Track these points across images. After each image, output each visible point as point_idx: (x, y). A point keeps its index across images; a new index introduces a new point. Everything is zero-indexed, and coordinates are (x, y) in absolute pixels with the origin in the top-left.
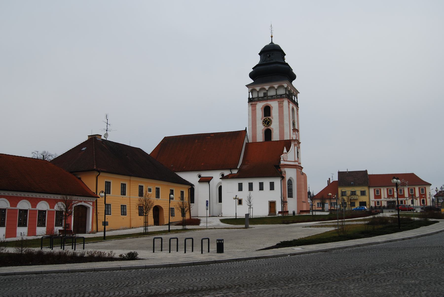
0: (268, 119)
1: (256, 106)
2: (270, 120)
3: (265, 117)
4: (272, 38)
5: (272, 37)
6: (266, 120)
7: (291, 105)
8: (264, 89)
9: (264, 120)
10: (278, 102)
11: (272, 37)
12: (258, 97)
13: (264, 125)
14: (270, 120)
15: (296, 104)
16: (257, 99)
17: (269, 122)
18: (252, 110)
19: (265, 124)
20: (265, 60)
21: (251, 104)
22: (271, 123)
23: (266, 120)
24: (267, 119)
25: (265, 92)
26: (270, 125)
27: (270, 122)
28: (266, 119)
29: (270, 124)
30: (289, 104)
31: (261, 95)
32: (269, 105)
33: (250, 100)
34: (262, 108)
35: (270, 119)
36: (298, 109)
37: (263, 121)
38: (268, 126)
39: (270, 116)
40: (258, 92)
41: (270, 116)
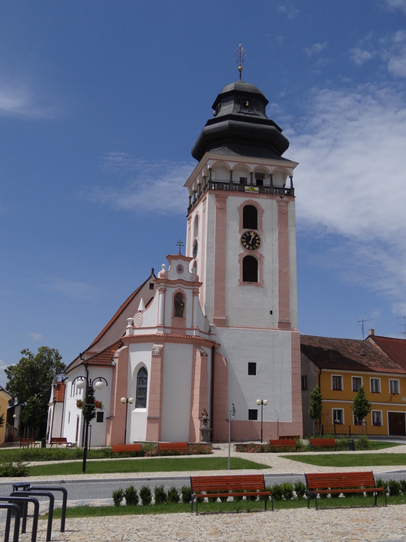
1: (226, 202)
6: (248, 235)
9: (245, 234)
10: (277, 201)
13: (245, 246)
18: (217, 208)
22: (259, 243)
23: (248, 235)
27: (257, 241)
28: (249, 233)
29: (257, 245)
34: (239, 209)
37: (243, 238)
38: (253, 249)
39: (256, 228)
40: (231, 171)
41: (256, 228)
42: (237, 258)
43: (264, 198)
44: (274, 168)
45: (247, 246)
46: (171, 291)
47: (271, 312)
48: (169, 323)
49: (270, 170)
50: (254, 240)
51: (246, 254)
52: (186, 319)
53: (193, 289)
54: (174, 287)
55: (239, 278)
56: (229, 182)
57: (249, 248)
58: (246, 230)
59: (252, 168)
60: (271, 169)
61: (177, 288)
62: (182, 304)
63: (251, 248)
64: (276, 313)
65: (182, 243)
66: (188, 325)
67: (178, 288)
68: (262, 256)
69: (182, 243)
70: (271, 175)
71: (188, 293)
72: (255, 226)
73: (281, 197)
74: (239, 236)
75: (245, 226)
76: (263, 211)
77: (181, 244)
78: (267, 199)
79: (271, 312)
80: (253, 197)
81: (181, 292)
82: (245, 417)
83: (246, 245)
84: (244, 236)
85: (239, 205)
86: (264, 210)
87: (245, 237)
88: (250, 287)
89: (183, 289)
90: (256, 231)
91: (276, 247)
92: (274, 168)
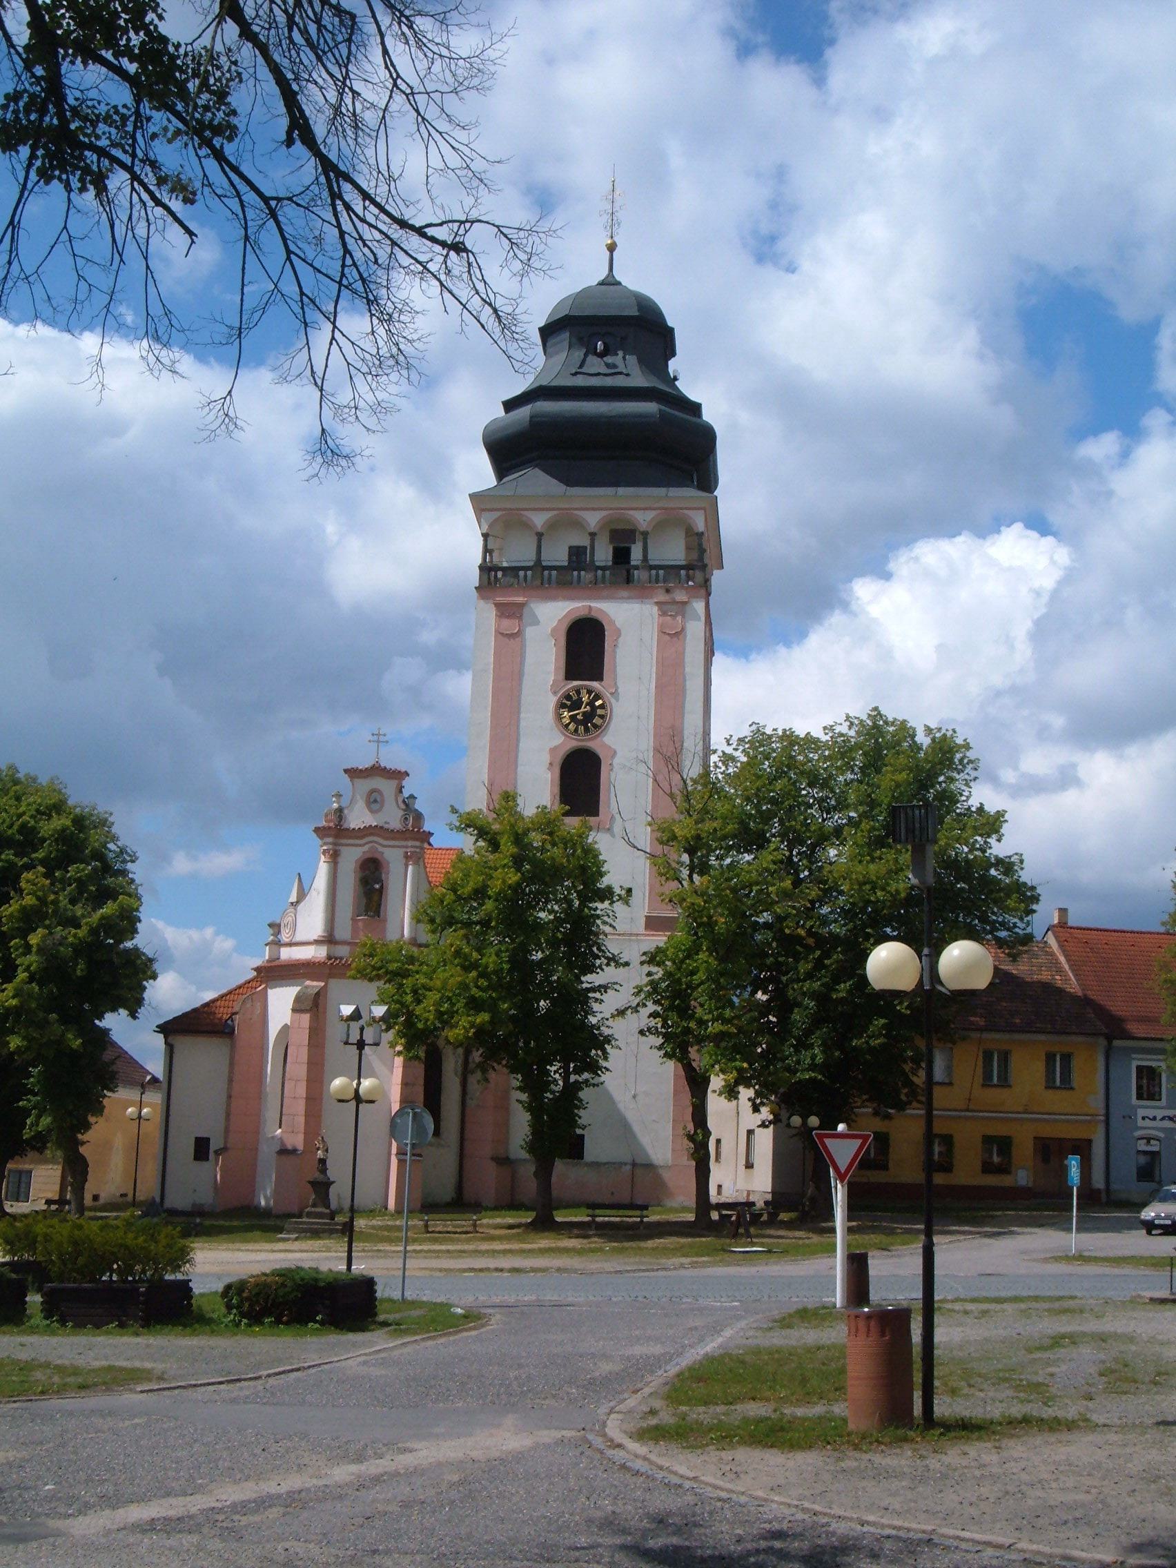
4: (615, 253)
5: (612, 248)
6: (575, 698)
8: (577, 524)
9: (568, 697)
11: (612, 248)
12: (539, 566)
16: (529, 573)
18: (500, 634)
20: (581, 367)
21: (497, 605)
23: (575, 698)
25: (582, 541)
27: (599, 712)
28: (578, 692)
29: (597, 720)
31: (557, 554)
32: (600, 618)
39: (599, 677)
40: (540, 536)
41: (599, 677)
42: (546, 758)
43: (623, 598)
44: (650, 515)
45: (572, 727)
46: (352, 855)
48: (344, 932)
49: (642, 521)
51: (573, 744)
52: (385, 921)
54: (360, 845)
56: (531, 564)
57: (576, 730)
59: (593, 519)
60: (643, 519)
61: (366, 848)
62: (377, 886)
63: (581, 728)
67: (371, 845)
69: (385, 735)
70: (645, 535)
71: (392, 855)
72: (597, 673)
73: (668, 591)
74: (552, 701)
75: (570, 675)
77: (382, 738)
78: (629, 598)
81: (377, 856)
84: (565, 701)
87: (569, 703)
89: (380, 849)
90: (595, 684)
92: (650, 515)
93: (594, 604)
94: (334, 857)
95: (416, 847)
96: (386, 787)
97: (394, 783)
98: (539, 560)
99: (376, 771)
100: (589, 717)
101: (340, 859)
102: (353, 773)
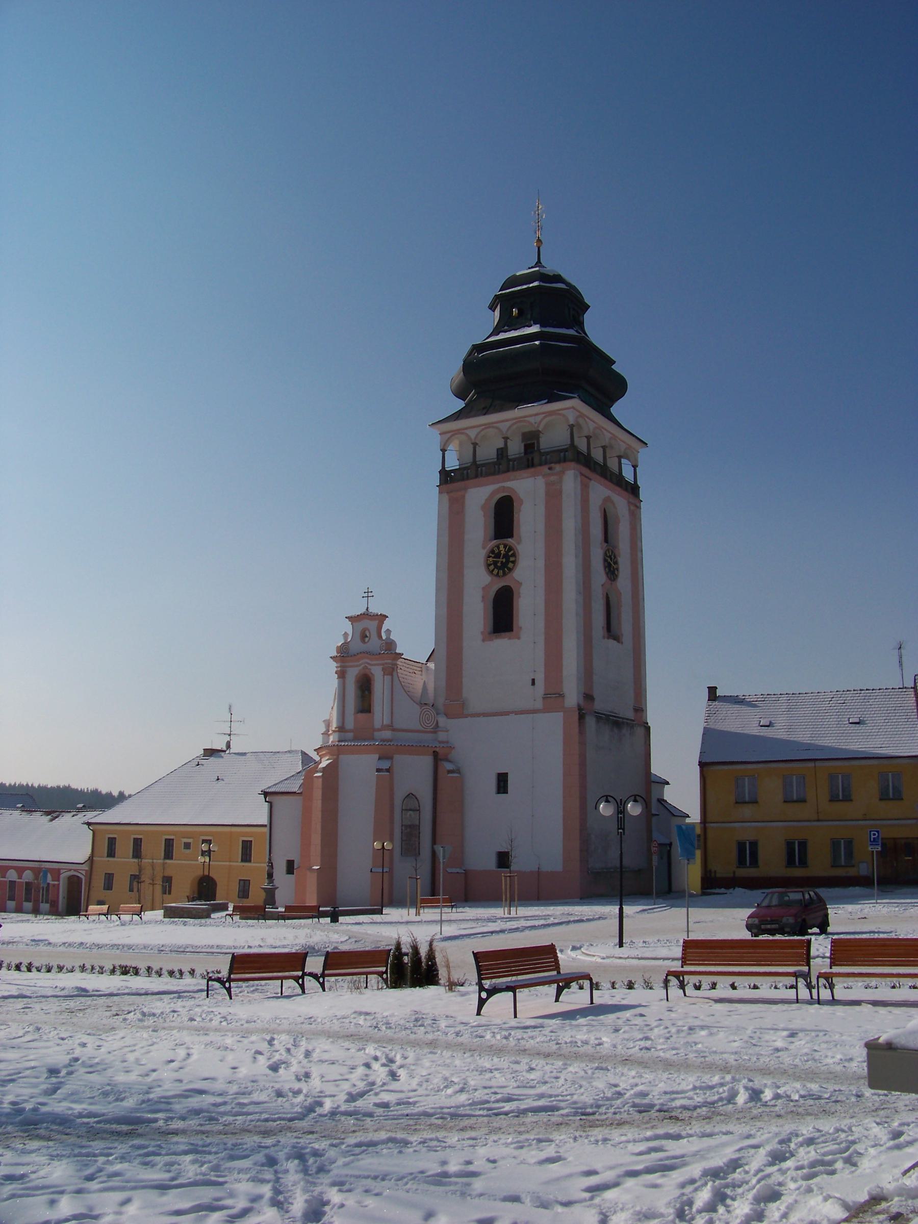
0: (505, 546)
2: (512, 552)
3: (495, 539)
6: (497, 551)
7: (600, 491)
9: (492, 551)
14: (512, 552)
15: (633, 490)
17: (506, 556)
19: (496, 567)
22: (514, 562)
23: (497, 551)
24: (502, 548)
26: (510, 570)
27: (512, 559)
29: (510, 565)
30: (585, 487)
33: (446, 477)
34: (484, 508)
35: (510, 549)
36: (639, 508)
38: (504, 574)
39: (511, 536)
41: (511, 536)
45: (496, 571)
46: (353, 674)
47: (533, 680)
48: (350, 724)
50: (506, 556)
53: (383, 664)
54: (357, 666)
55: (482, 630)
58: (495, 542)
63: (501, 572)
64: (540, 683)
65: (371, 592)
66: (377, 724)
68: (519, 584)
69: (371, 592)
71: (377, 673)
73: (550, 469)
74: (483, 553)
76: (521, 502)
77: (370, 594)
79: (533, 680)
80: (504, 481)
82: (491, 863)
83: (493, 570)
85: (483, 502)
86: (522, 501)
88: (502, 643)
89: (369, 667)
90: (510, 541)
91: (541, 563)
93: (508, 484)
94: (342, 674)
95: (389, 664)
96: (372, 625)
97: (375, 623)
98: (474, 461)
99: (366, 615)
100: (504, 565)
101: (347, 676)
102: (352, 619)
